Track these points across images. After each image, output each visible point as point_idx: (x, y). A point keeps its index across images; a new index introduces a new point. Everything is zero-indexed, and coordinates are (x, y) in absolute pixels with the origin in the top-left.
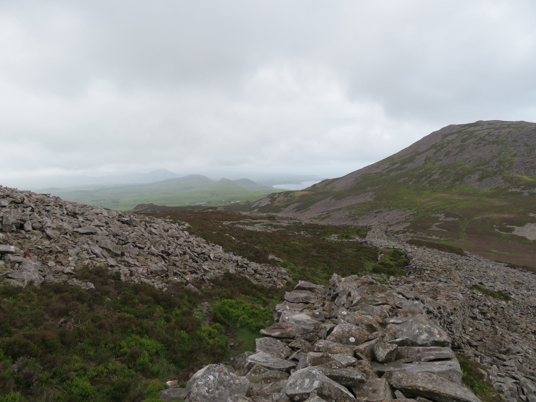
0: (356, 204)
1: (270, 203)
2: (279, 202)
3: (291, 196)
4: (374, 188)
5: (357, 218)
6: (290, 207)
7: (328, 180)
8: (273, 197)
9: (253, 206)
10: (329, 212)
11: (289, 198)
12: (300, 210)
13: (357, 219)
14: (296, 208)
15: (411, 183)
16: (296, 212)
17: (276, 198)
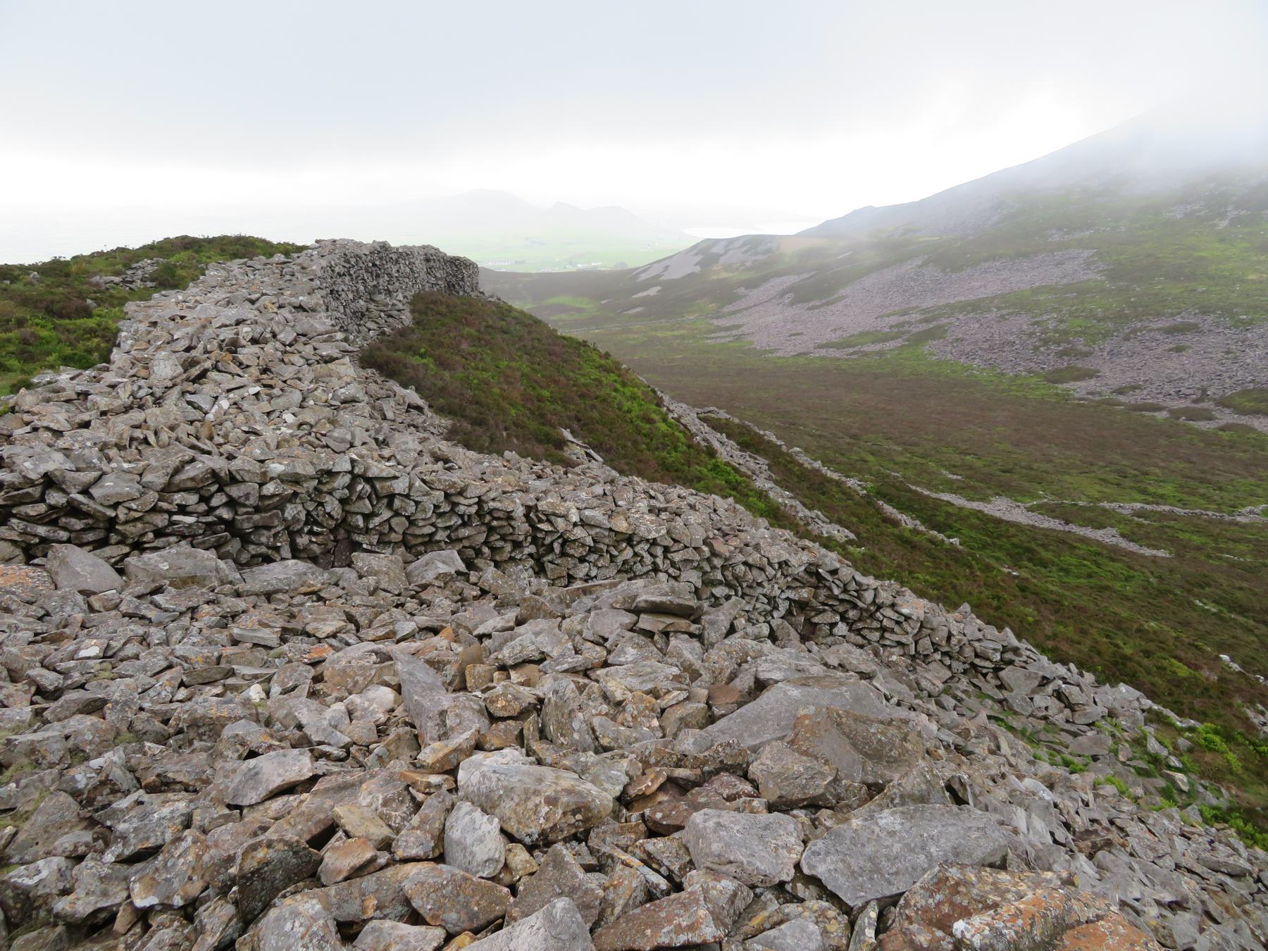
0: (1036, 291)
1: (698, 269)
2: (728, 268)
3: (768, 251)
4: (1078, 235)
5: (1086, 349)
6: (767, 286)
7: (869, 209)
8: (707, 253)
9: (643, 277)
10: (930, 316)
11: (760, 257)
12: (808, 301)
13: (1087, 354)
14: (789, 290)
15: (1225, 223)
16: (792, 304)
17: (718, 256)
